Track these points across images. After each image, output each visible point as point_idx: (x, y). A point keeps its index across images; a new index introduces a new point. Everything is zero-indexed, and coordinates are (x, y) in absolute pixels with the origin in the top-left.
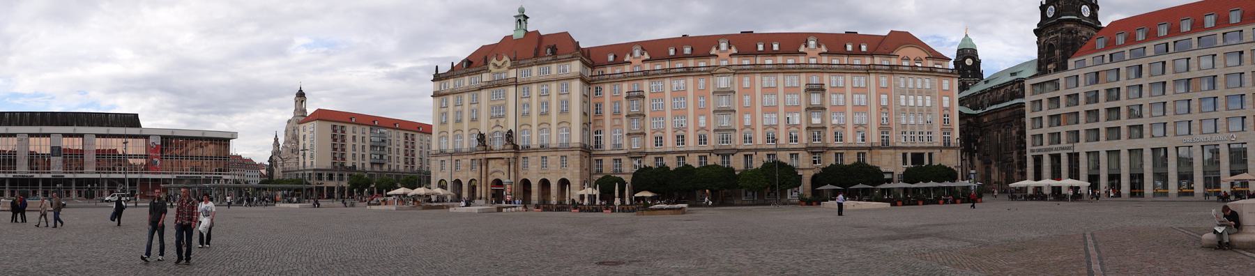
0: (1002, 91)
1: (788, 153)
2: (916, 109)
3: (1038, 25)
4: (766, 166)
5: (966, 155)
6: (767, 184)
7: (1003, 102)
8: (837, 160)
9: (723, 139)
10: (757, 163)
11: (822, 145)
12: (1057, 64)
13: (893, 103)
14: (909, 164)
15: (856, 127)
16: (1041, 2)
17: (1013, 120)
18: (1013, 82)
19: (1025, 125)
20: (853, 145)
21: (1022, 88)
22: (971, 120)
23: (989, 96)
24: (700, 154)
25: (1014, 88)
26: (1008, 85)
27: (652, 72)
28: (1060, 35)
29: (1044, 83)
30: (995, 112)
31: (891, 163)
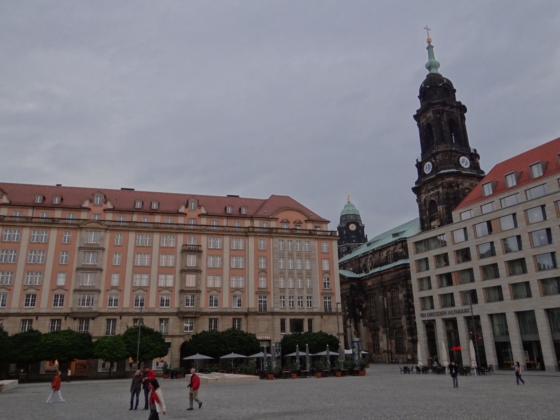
0: (384, 253)
1: (157, 318)
2: (295, 272)
3: (416, 183)
4: (131, 333)
5: (350, 321)
6: (128, 353)
7: (386, 263)
8: (210, 326)
9: (84, 300)
10: (120, 330)
11: (195, 310)
12: (441, 221)
13: (272, 266)
14: (288, 332)
15: (233, 290)
16: (417, 160)
17: (399, 283)
18: (396, 243)
19: (411, 287)
20: (229, 311)
21: (405, 248)
22: (354, 284)
23: (371, 259)
24: (52, 318)
25: (397, 248)
26: (390, 246)
27: (9, 219)
28: (441, 190)
29: (427, 239)
30: (378, 275)
31: (268, 330)
